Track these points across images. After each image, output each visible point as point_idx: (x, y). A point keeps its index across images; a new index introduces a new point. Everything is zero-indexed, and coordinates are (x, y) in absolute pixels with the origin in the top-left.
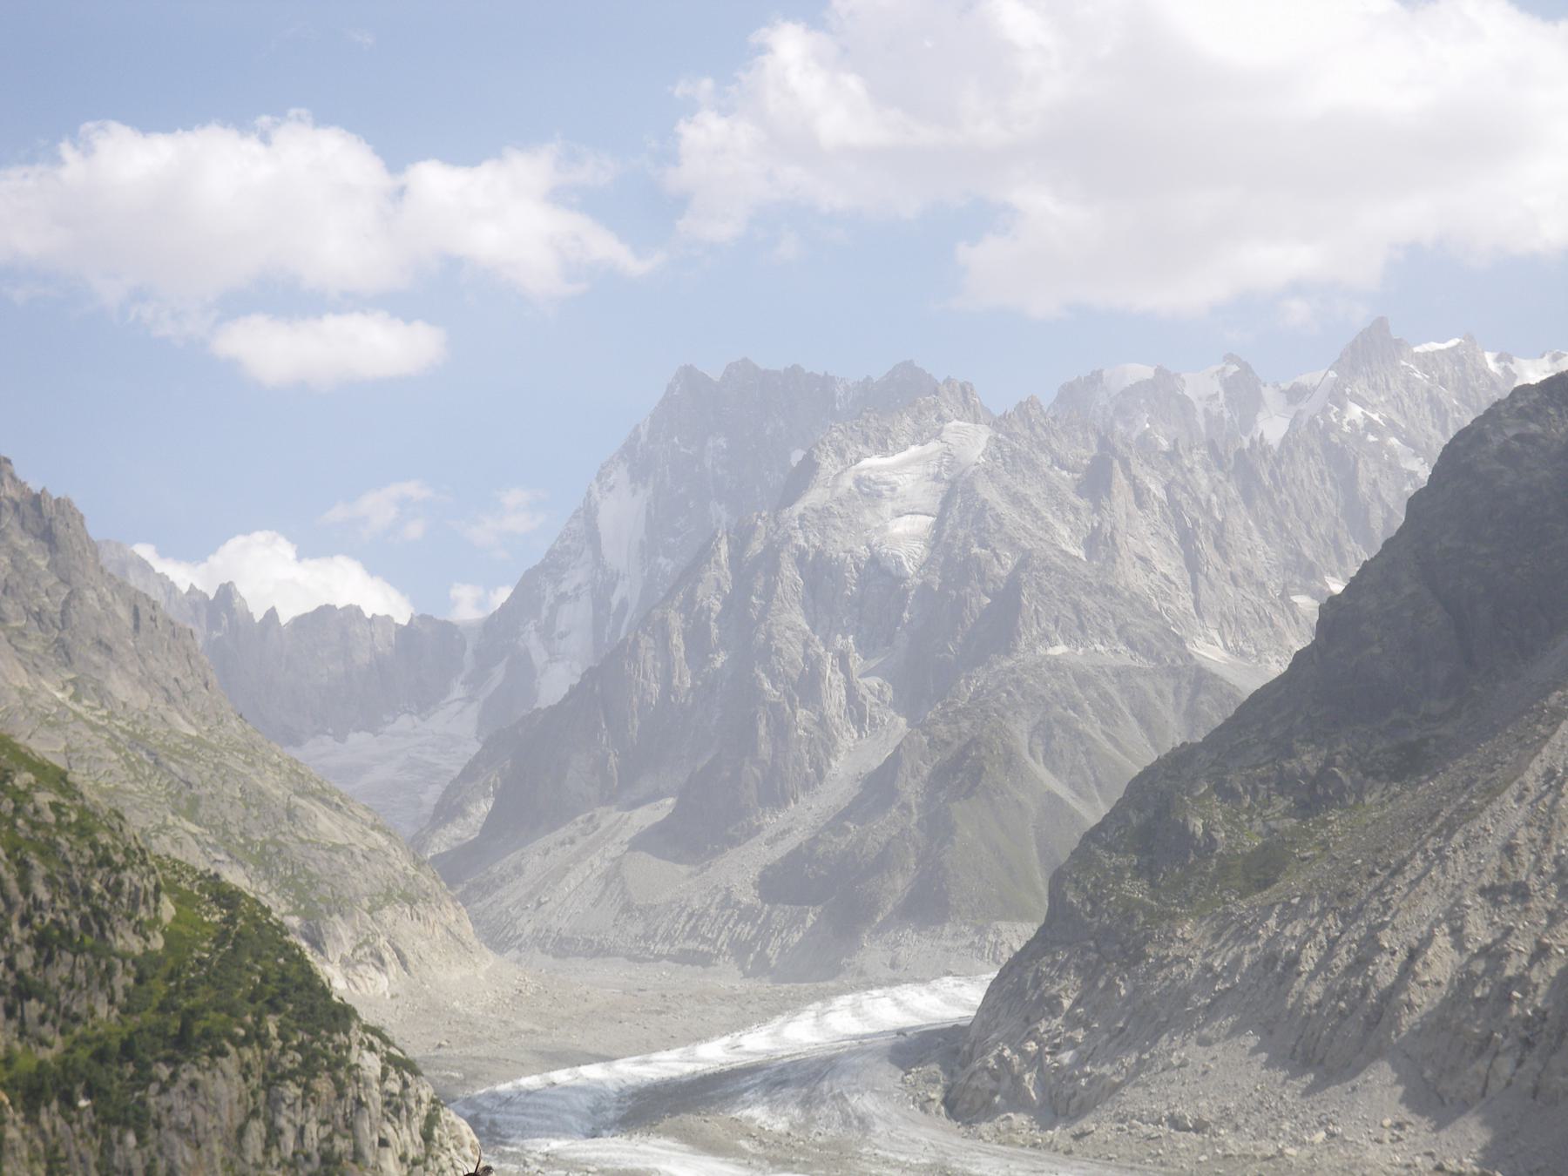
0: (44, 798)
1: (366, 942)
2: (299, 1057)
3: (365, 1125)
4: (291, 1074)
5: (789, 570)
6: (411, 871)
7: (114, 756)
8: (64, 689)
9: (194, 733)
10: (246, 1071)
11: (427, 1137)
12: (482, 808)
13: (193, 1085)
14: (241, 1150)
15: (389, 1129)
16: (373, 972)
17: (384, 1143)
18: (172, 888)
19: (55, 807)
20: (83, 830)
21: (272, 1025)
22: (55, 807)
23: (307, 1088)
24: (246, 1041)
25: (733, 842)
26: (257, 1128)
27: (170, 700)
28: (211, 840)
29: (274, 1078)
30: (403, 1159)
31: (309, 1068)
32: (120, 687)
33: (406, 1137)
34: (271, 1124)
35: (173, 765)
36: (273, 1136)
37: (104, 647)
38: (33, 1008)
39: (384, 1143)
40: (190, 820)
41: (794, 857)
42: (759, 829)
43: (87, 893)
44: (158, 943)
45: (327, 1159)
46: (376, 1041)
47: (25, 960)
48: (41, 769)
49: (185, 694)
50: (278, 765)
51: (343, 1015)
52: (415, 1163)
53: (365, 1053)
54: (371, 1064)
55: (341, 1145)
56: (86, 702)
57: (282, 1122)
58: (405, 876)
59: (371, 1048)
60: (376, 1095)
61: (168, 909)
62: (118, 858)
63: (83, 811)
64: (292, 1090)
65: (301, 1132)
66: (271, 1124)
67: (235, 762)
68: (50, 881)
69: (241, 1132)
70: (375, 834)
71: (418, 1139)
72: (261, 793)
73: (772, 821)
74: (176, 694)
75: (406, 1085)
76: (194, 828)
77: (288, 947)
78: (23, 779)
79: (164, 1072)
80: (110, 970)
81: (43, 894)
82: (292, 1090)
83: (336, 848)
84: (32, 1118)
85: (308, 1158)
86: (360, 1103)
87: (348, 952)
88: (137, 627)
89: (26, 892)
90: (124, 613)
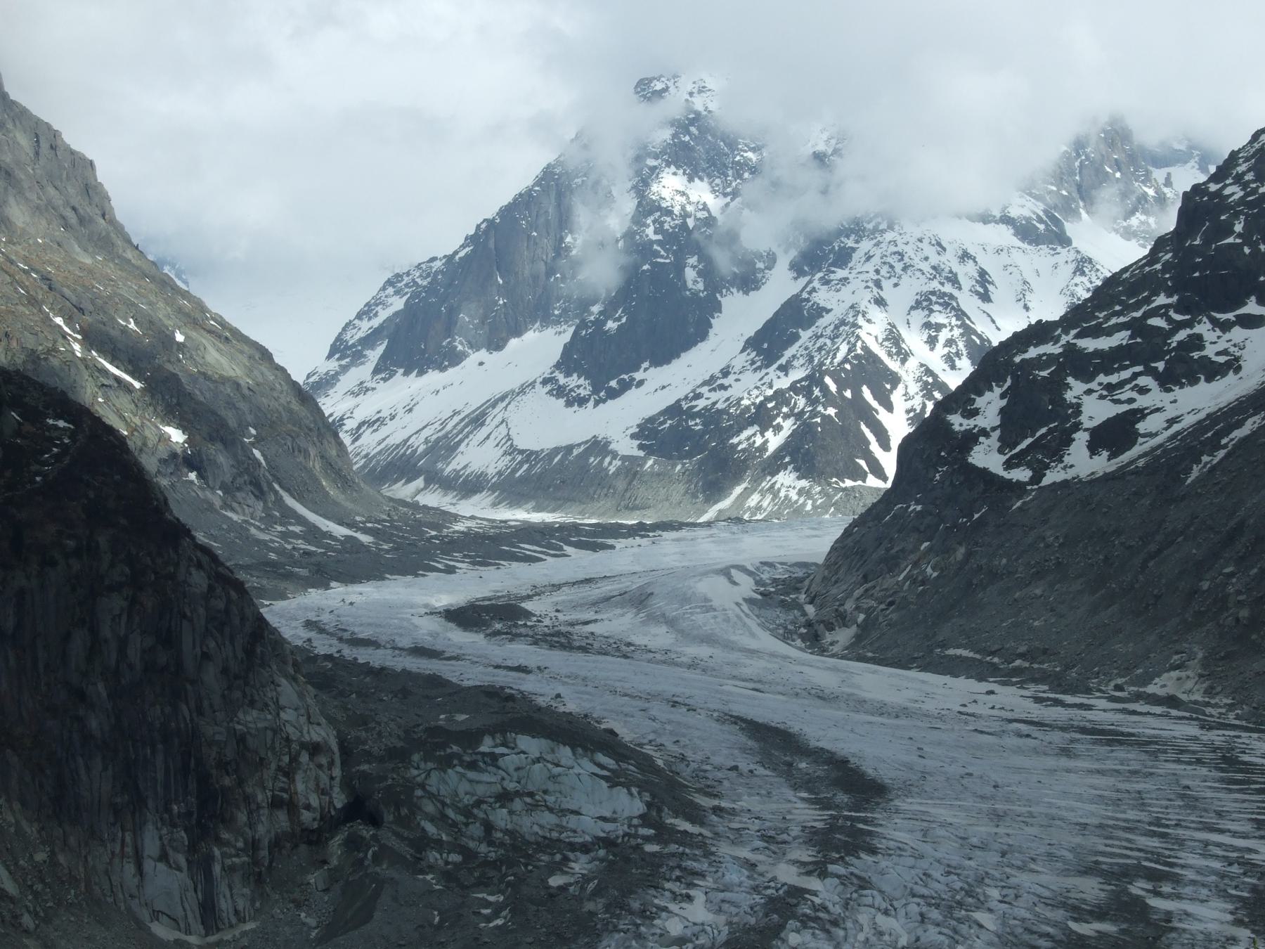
1: (247, 470)
2: (127, 570)
11: (249, 652)
15: (212, 644)
16: (251, 500)
17: (206, 656)
21: (103, 541)
30: (225, 671)
39: (206, 656)
41: (674, 410)
42: (641, 383)
46: (205, 559)
52: (236, 677)
53: (193, 570)
54: (199, 580)
57: (106, 632)
58: (290, 411)
59: (199, 566)
60: (201, 611)
64: (117, 603)
65: (123, 643)
71: (240, 654)
73: (652, 376)
74: (73, 219)
75: (229, 601)
82: (117, 603)
85: (131, 667)
86: (184, 616)
87: (228, 478)
88: (37, 154)
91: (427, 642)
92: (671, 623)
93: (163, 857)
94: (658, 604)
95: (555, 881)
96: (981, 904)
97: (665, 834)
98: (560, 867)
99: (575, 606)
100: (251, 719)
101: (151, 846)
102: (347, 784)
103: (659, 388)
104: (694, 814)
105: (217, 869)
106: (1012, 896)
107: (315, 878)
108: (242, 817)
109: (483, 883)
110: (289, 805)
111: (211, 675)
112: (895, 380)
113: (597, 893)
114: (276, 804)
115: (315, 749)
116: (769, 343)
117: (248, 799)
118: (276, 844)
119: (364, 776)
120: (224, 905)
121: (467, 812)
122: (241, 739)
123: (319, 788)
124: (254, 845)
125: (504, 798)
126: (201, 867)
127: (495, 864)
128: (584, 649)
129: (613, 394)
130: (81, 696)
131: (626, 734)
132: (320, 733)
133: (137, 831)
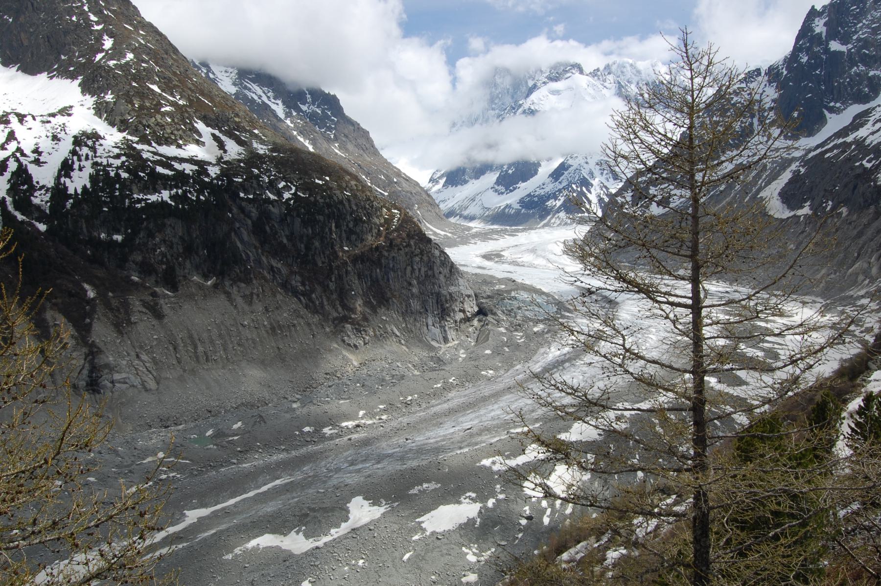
0: (353, 183)
3: (435, 268)
4: (417, 255)
10: (406, 254)
11: (451, 271)
13: (393, 257)
14: (405, 274)
17: (440, 273)
19: (356, 185)
20: (363, 192)
21: (412, 243)
22: (356, 185)
23: (421, 258)
24: (406, 246)
26: (409, 268)
29: (412, 255)
31: (422, 253)
32: (350, 147)
33: (446, 271)
34: (412, 267)
36: (413, 270)
38: (353, 237)
39: (440, 273)
41: (529, 195)
43: (365, 208)
44: (382, 221)
45: (426, 276)
47: (351, 225)
48: (350, 174)
51: (429, 240)
54: (437, 253)
55: (430, 273)
62: (372, 199)
63: (363, 186)
64: (417, 259)
65: (420, 270)
66: (412, 267)
68: (356, 205)
69: (405, 269)
73: (522, 185)
77: (414, 223)
78: (347, 178)
79: (386, 254)
80: (371, 229)
81: (355, 208)
83: (407, 192)
84: (355, 266)
89: (351, 207)
91: (480, 265)
92: (544, 257)
93: (433, 325)
94: (539, 252)
95: (536, 329)
96: (650, 333)
97: (563, 317)
98: (534, 326)
99: (516, 253)
100: (452, 289)
101: (430, 323)
102: (478, 305)
103: (525, 188)
104: (569, 311)
105: (447, 328)
106: (658, 331)
107: (470, 329)
108: (452, 314)
109: (516, 330)
110: (463, 311)
111: (442, 277)
112: (592, 185)
113: (547, 333)
114: (460, 311)
115: (469, 296)
116: (556, 175)
117: (453, 310)
118: (461, 322)
119: (482, 303)
120: (450, 337)
121: (510, 311)
122: (450, 294)
123: (471, 307)
124: (456, 322)
125: (519, 308)
126: (443, 327)
127: (519, 325)
128: (523, 266)
129: (511, 191)
130: (410, 284)
131: (545, 290)
132: (470, 292)
133: (426, 318)
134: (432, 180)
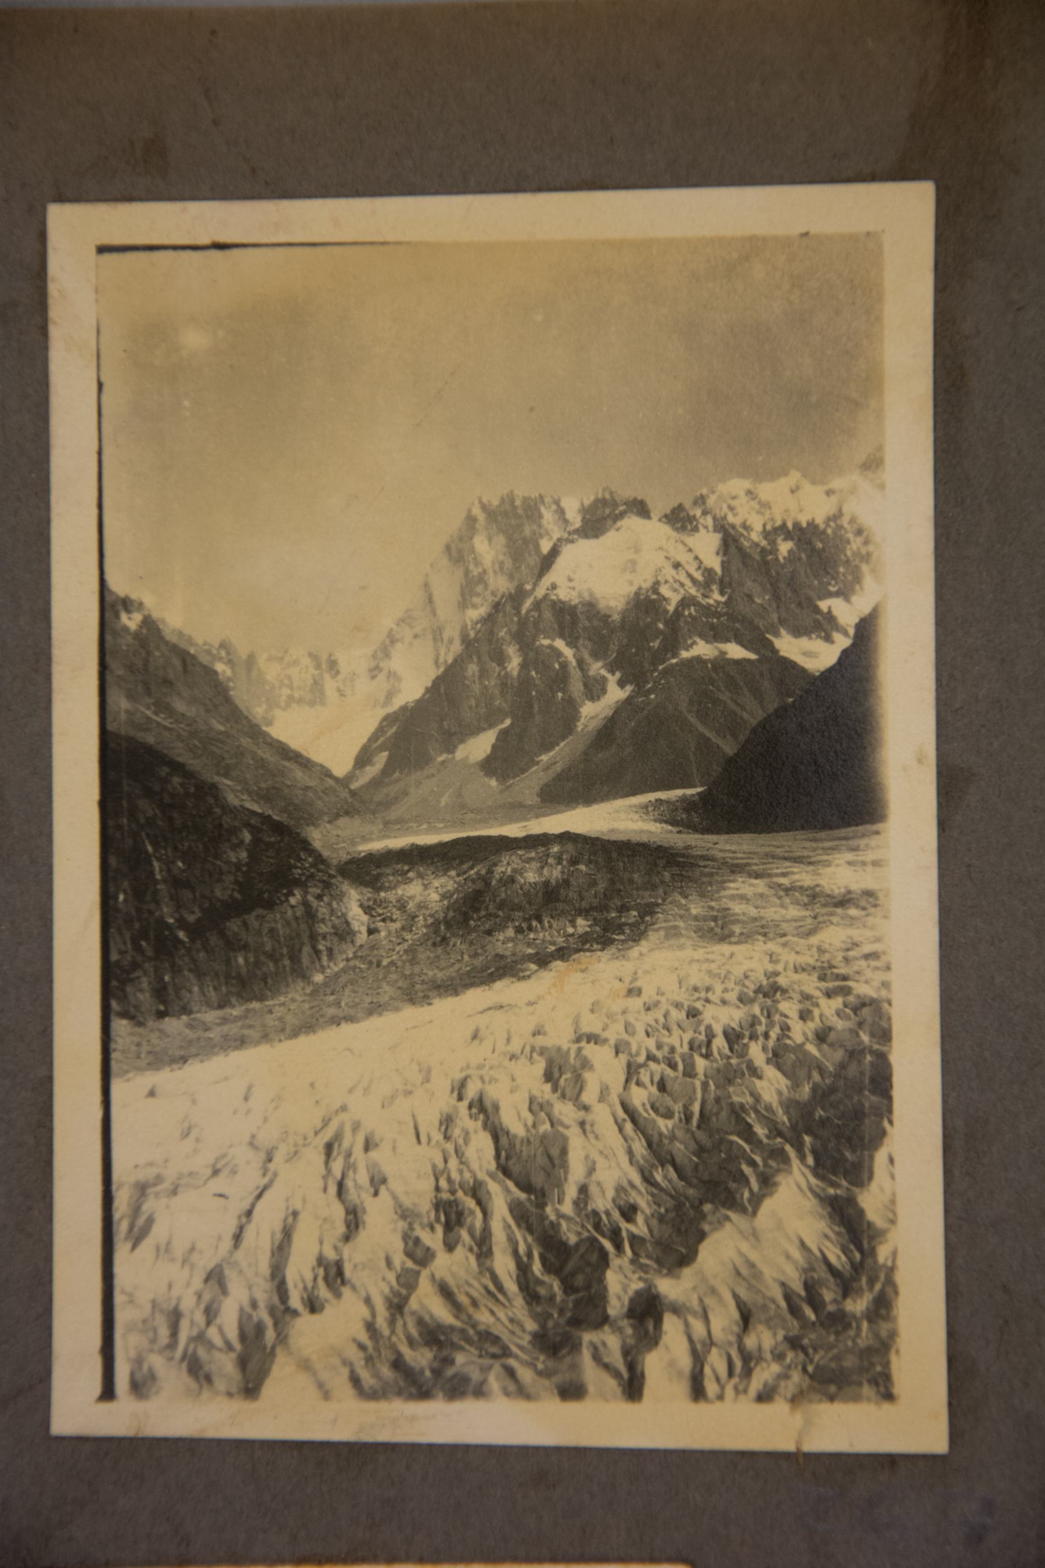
0: (176, 780)
5: (548, 615)
6: (350, 800)
7: (181, 745)
8: (148, 708)
9: (222, 728)
12: (381, 759)
18: (247, 825)
19: (182, 785)
22: (182, 785)
25: (523, 771)
27: (208, 711)
28: (239, 788)
32: (180, 706)
35: (215, 749)
37: (167, 682)
40: (226, 778)
49: (216, 706)
50: (271, 744)
56: (162, 716)
57: (321, 947)
61: (247, 837)
67: (246, 742)
70: (328, 779)
72: (262, 759)
76: (229, 782)
90: (176, 662)
134: (363, 759)
